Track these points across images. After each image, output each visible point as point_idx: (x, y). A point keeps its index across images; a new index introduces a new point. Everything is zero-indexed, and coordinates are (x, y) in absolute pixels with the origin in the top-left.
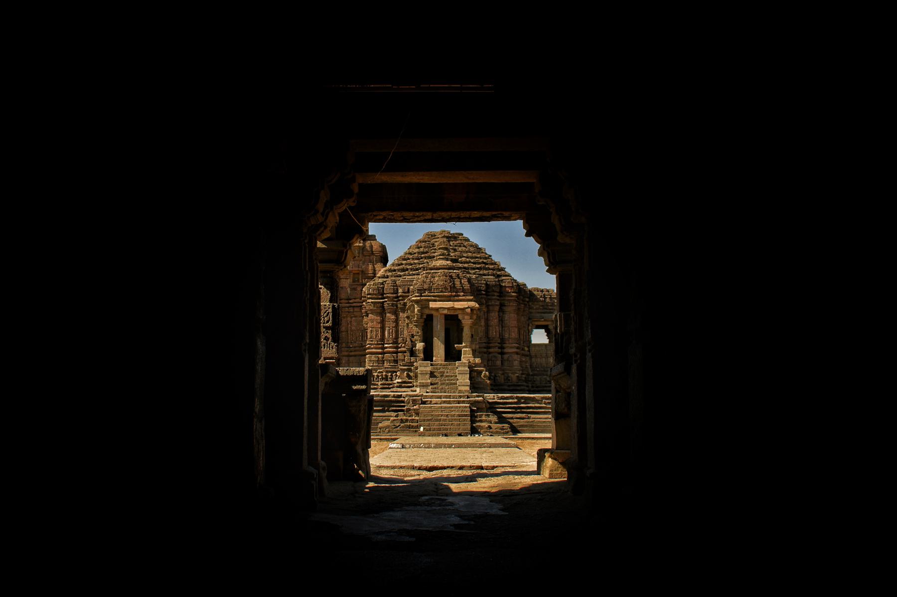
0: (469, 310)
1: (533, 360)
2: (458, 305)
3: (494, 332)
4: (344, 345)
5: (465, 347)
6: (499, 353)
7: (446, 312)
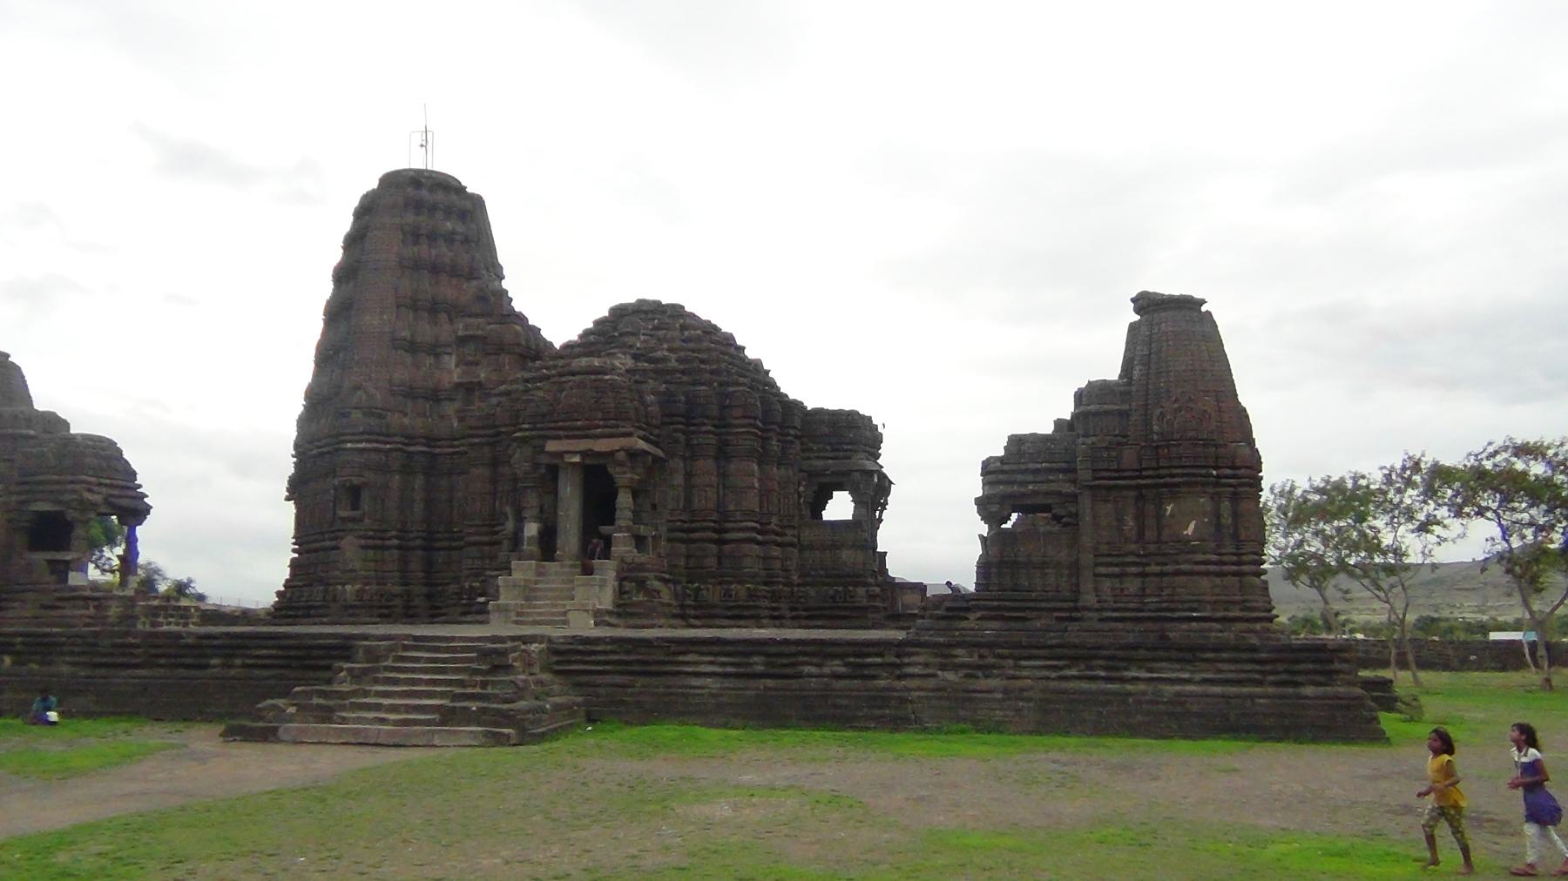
0: (621, 456)
2: (602, 445)
5: (620, 530)
7: (577, 459)
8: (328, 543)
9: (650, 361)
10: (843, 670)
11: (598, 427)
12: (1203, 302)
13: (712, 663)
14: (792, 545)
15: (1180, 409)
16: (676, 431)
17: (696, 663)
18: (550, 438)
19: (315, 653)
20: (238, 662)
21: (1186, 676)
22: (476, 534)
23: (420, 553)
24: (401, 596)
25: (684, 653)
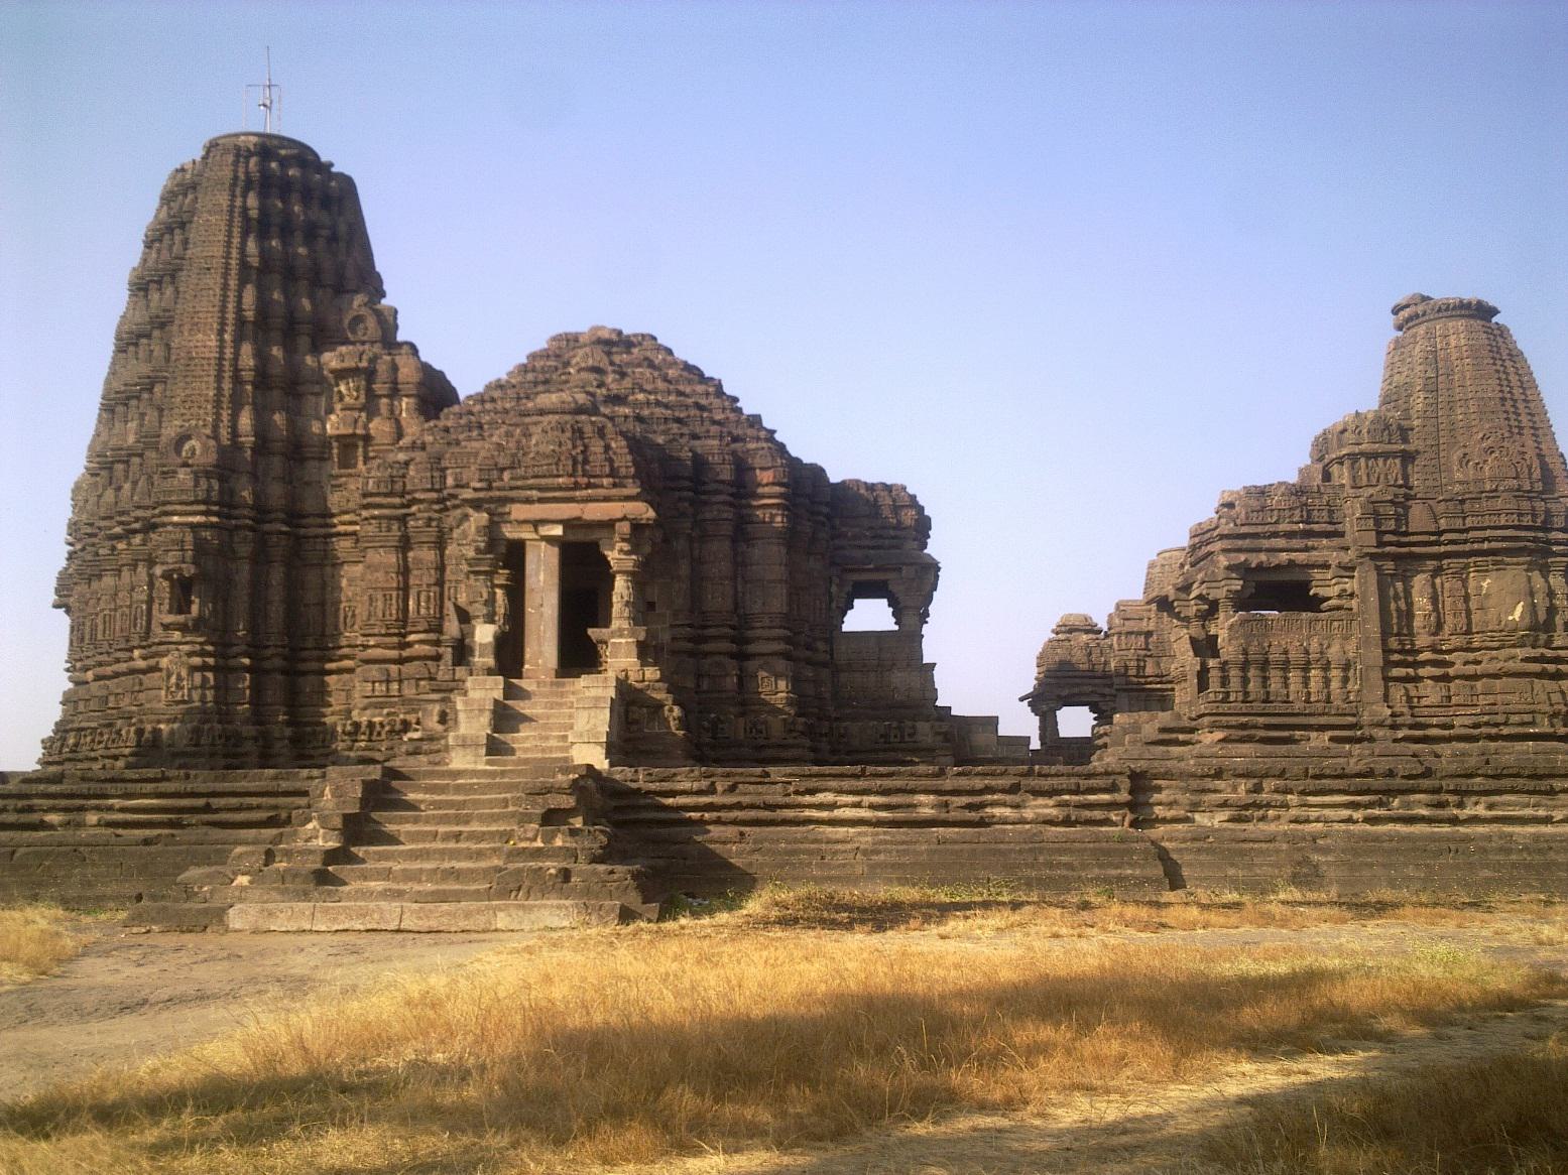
0: (624, 528)
1: (843, 677)
2: (595, 512)
3: (717, 599)
4: (310, 643)
5: (620, 633)
6: (732, 656)
7: (558, 531)
8: (141, 664)
10: (1054, 812)
12: (1494, 311)
13: (857, 805)
14: (825, 665)
15: (1490, 450)
16: (680, 499)
17: (833, 806)
18: (513, 500)
19: (216, 802)
20: (92, 818)
21: (1541, 813)
23: (280, 677)
24: (256, 739)
25: (812, 792)
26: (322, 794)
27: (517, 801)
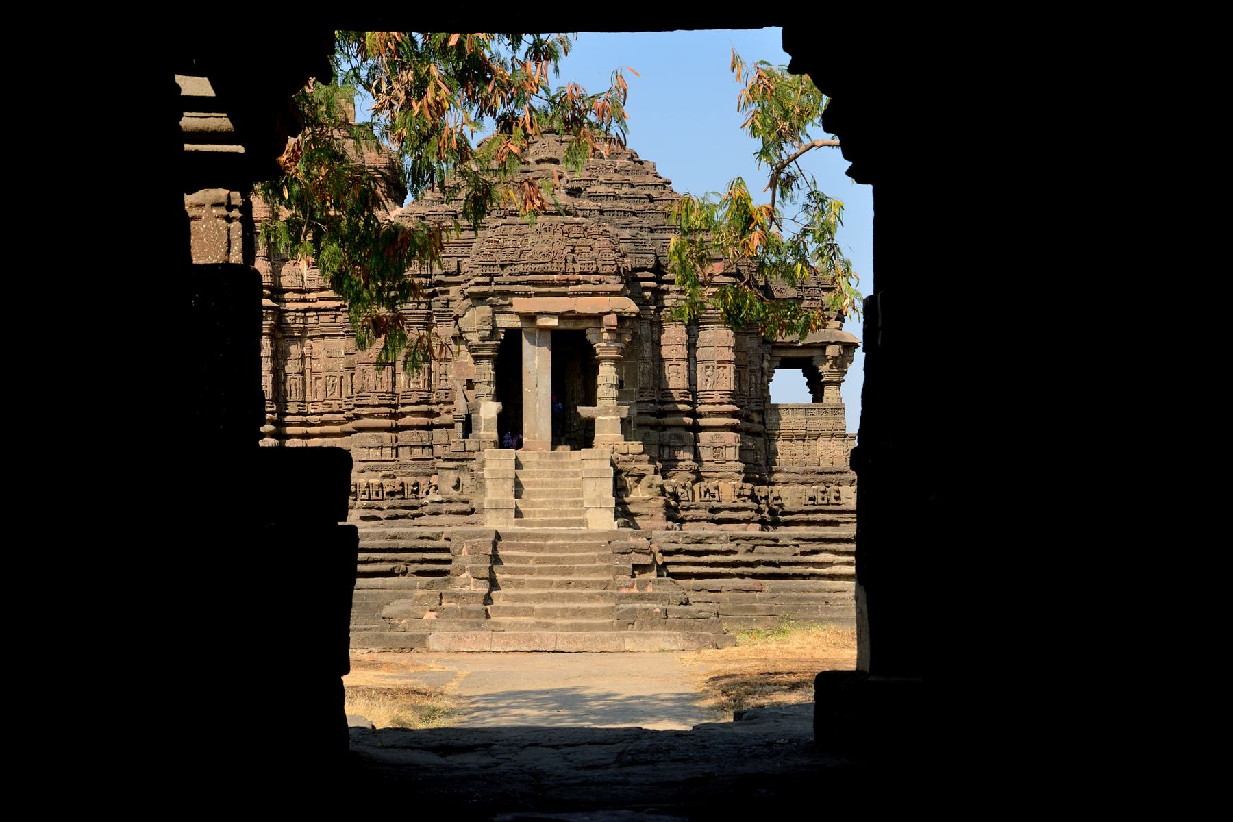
0: (611, 320)
5: (606, 411)
7: (554, 322)
9: (594, 197)
11: (578, 282)
14: (758, 434)
18: (513, 294)
22: (370, 416)
26: (460, 552)
27: (602, 558)
